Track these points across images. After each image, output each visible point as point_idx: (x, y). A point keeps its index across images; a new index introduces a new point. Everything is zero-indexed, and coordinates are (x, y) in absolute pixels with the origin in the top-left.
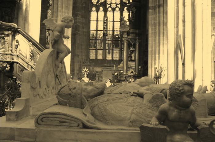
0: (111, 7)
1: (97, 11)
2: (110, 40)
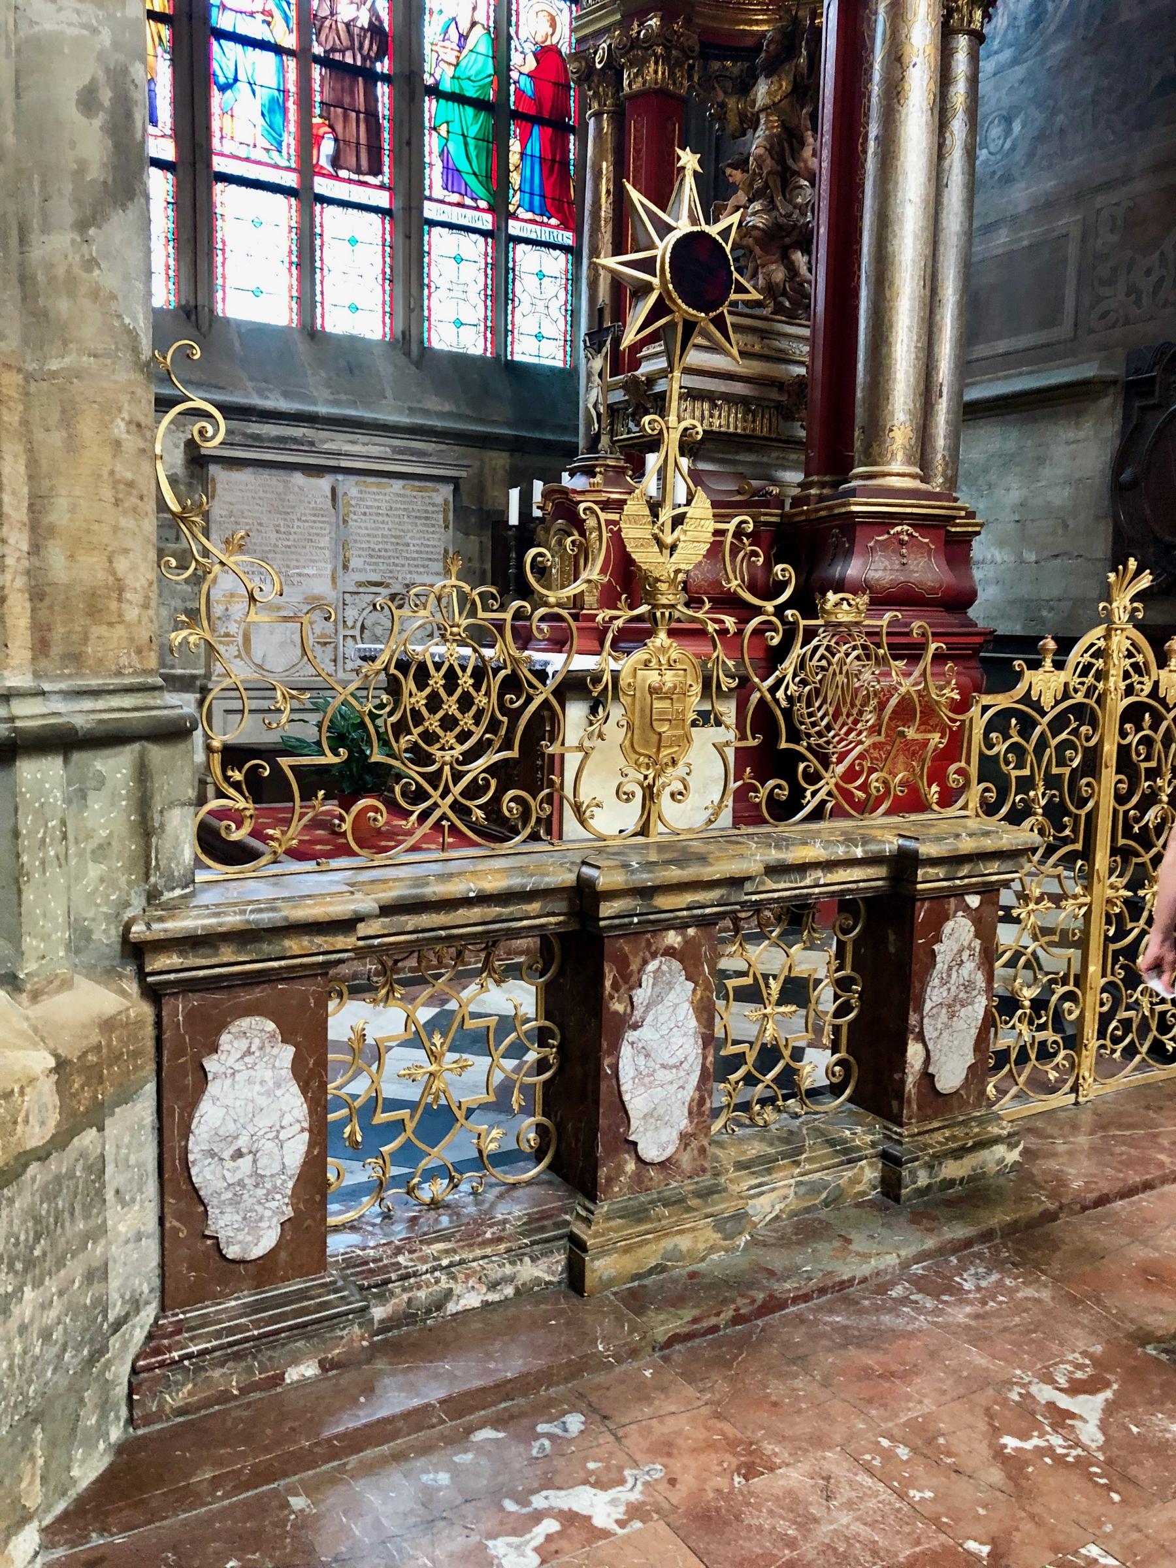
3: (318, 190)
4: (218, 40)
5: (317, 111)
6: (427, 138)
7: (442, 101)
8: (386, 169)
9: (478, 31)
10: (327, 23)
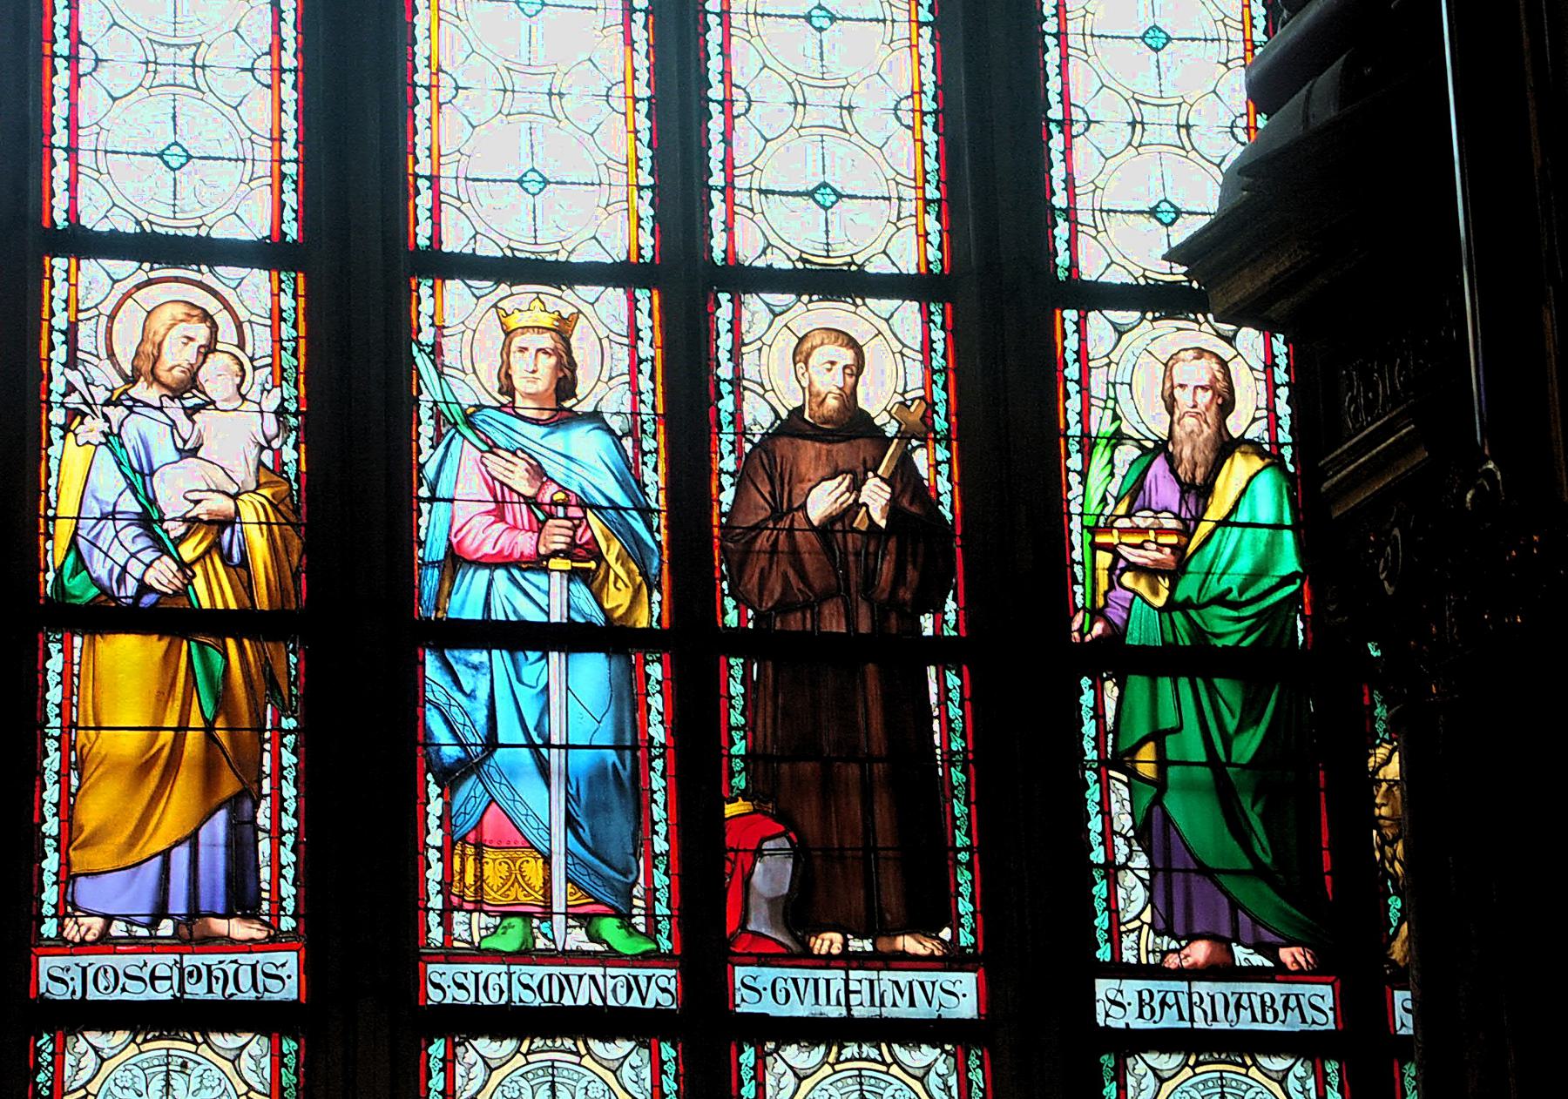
3: (747, 1003)
5: (740, 782)
6: (1093, 794)
7: (1138, 684)
8: (965, 907)
9: (1239, 468)
10: (763, 542)
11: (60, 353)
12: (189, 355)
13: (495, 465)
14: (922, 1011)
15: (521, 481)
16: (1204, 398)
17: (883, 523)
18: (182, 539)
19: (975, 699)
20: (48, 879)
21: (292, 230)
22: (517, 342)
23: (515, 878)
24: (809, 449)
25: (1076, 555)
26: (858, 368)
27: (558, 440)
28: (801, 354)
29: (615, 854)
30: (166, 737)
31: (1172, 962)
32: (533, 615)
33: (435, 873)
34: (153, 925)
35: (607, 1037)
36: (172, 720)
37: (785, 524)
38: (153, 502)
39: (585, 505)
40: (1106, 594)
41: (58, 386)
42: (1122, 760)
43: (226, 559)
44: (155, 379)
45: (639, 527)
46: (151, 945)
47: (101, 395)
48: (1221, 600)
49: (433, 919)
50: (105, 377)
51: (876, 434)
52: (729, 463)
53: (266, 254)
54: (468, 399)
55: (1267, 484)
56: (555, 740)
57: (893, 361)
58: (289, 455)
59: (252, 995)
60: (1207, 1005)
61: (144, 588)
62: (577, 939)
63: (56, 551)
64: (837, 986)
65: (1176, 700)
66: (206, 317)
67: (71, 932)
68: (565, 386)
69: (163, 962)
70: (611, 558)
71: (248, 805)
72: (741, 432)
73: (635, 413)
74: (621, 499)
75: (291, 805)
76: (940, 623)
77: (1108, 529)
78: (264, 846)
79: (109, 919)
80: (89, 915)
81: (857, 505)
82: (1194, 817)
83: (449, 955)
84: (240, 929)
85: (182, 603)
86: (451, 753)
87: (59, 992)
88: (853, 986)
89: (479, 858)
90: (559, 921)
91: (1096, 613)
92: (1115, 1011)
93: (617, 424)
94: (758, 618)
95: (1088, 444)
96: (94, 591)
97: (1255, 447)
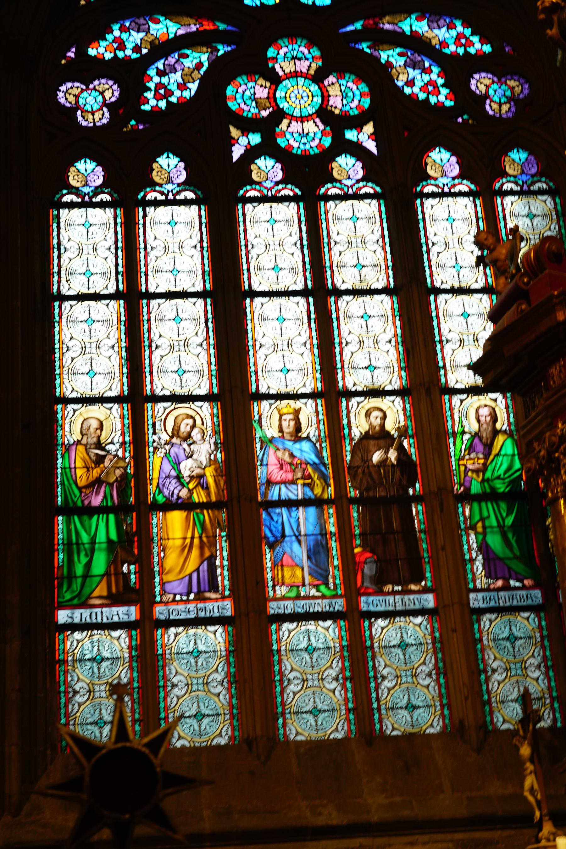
0: (283, 156)
1: (128, 194)
2: (305, 503)
4: (266, 510)
5: (358, 542)
6: (464, 538)
7: (475, 505)
8: (428, 575)
9: (501, 438)
10: (360, 471)
11: (151, 431)
12: (188, 428)
13: (279, 454)
14: (417, 606)
15: (287, 458)
16: (488, 419)
17: (395, 463)
18: (188, 483)
19: (426, 513)
20: (157, 584)
21: (215, 390)
22: (284, 417)
23: (293, 575)
24: (372, 442)
25: (454, 468)
26: (384, 417)
27: (297, 446)
28: (368, 414)
29: (322, 565)
30: (188, 541)
31: (492, 587)
32: (293, 497)
33: (269, 575)
34: (188, 595)
35: (324, 620)
36: (189, 535)
37: (367, 464)
38: (180, 472)
39: (307, 463)
40: (464, 479)
41: (151, 440)
42: (473, 527)
43: (203, 487)
44: (178, 436)
45: (323, 469)
46: (188, 601)
47: (163, 442)
48: (498, 478)
49: (270, 589)
50: (165, 437)
51: (392, 437)
52: (348, 448)
53: (208, 398)
54: (269, 436)
55: (509, 442)
56: (303, 533)
57: (395, 414)
58: (219, 455)
59: (218, 615)
60: (503, 598)
61: (179, 497)
62: (313, 592)
63: (152, 489)
64: (392, 600)
65: (488, 509)
66: (192, 417)
67: (164, 599)
68: (298, 428)
69: (191, 606)
70: (315, 479)
71: (213, 559)
72: (352, 439)
73: (319, 436)
74: (317, 461)
75: (226, 558)
76: (414, 490)
77: (463, 459)
78: (219, 571)
79: (175, 595)
80: (169, 593)
81: (387, 458)
82: (495, 541)
83: (275, 599)
84: (213, 596)
85: (190, 501)
86: (272, 539)
87: (162, 617)
88: (396, 600)
89: (282, 570)
90: (307, 587)
91: (461, 485)
92: (476, 603)
93: (314, 440)
94: (360, 493)
95: (454, 435)
96: (164, 499)
97: (505, 432)
